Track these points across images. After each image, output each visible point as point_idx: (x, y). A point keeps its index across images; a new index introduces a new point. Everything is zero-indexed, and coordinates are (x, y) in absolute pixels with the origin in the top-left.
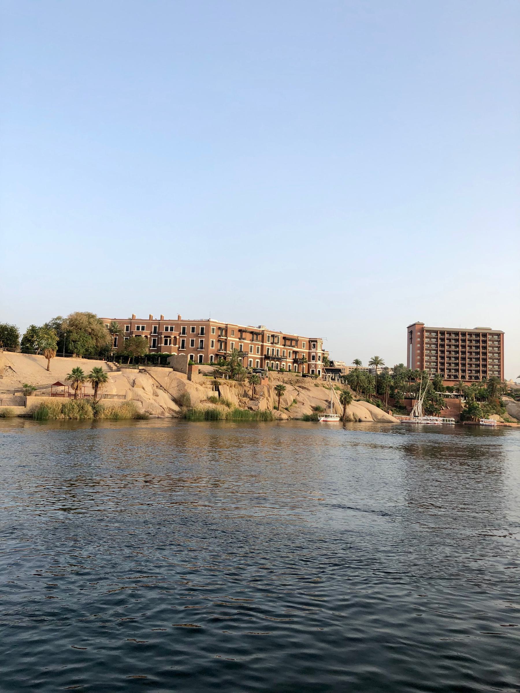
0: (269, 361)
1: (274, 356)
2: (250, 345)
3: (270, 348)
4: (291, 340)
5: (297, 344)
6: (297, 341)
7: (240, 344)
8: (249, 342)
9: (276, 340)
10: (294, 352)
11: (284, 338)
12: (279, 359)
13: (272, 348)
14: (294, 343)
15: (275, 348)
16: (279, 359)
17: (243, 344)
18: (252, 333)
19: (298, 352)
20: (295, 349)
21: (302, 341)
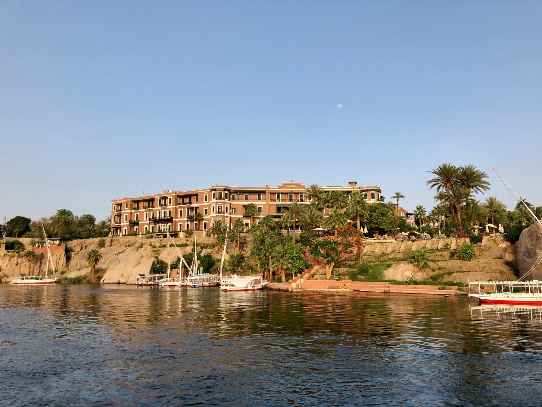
0: (160, 225)
1: (166, 218)
2: (145, 213)
3: (161, 211)
4: (190, 196)
5: (197, 200)
6: (197, 195)
7: (136, 214)
8: (143, 210)
9: (162, 202)
10: (192, 209)
11: (180, 197)
12: (170, 220)
13: (163, 211)
14: (194, 199)
15: (166, 210)
16: (170, 220)
17: (138, 213)
18: (145, 201)
19: (198, 208)
20: (192, 205)
21: (203, 194)
